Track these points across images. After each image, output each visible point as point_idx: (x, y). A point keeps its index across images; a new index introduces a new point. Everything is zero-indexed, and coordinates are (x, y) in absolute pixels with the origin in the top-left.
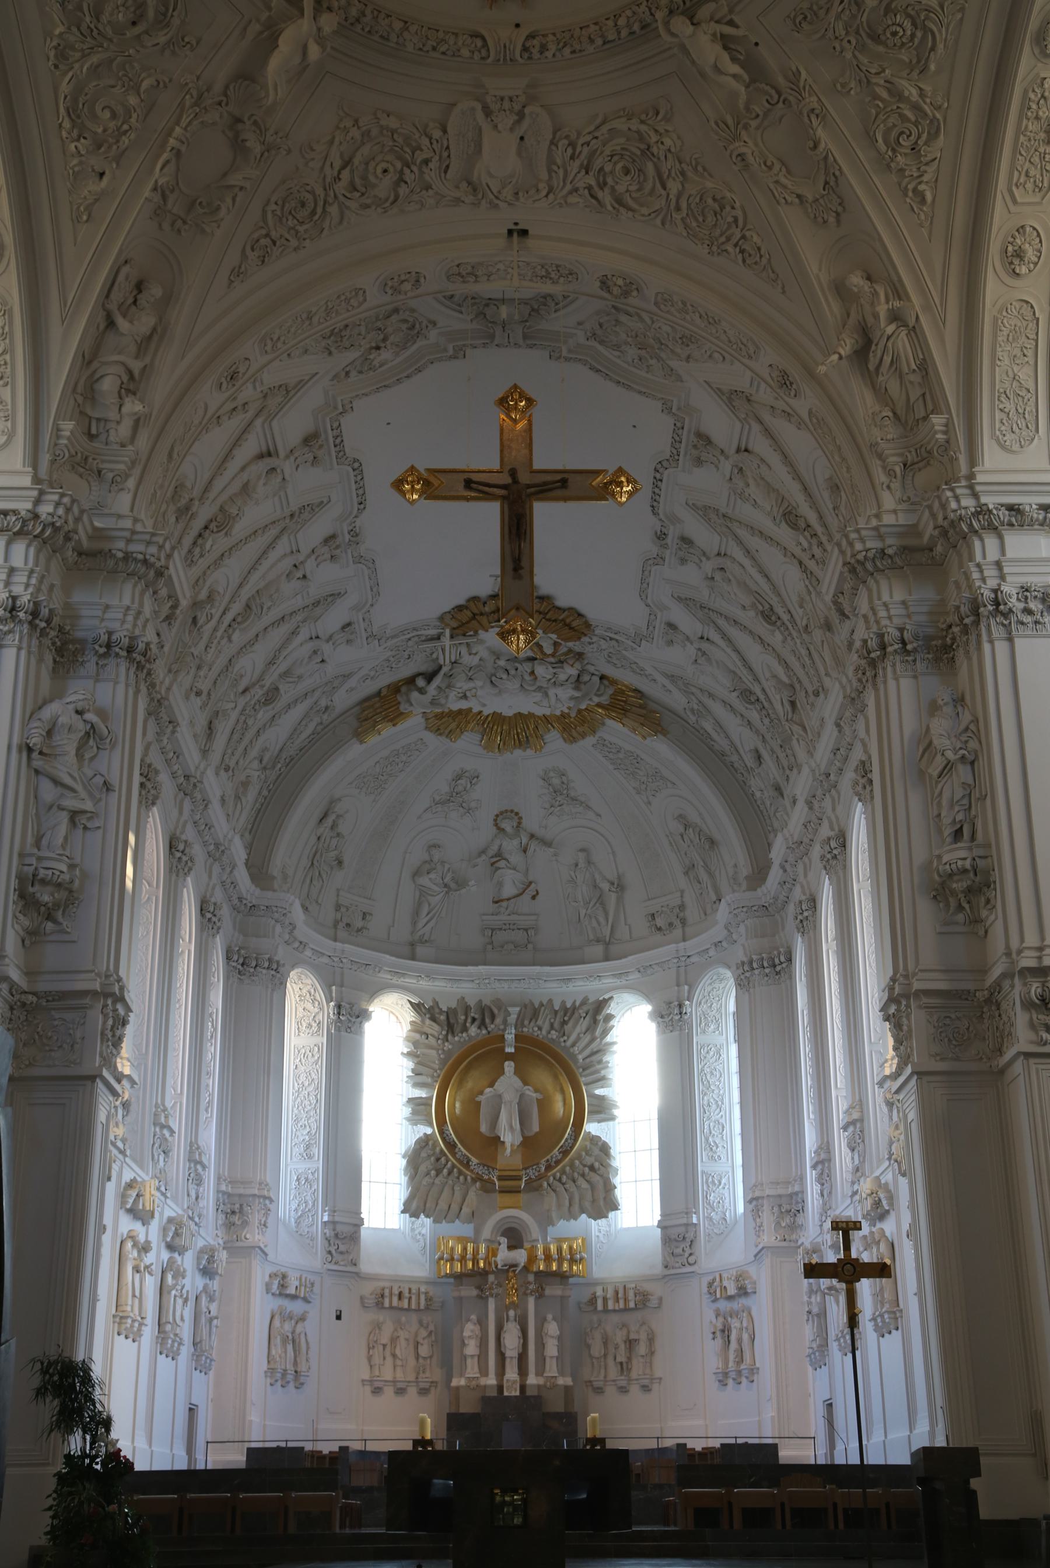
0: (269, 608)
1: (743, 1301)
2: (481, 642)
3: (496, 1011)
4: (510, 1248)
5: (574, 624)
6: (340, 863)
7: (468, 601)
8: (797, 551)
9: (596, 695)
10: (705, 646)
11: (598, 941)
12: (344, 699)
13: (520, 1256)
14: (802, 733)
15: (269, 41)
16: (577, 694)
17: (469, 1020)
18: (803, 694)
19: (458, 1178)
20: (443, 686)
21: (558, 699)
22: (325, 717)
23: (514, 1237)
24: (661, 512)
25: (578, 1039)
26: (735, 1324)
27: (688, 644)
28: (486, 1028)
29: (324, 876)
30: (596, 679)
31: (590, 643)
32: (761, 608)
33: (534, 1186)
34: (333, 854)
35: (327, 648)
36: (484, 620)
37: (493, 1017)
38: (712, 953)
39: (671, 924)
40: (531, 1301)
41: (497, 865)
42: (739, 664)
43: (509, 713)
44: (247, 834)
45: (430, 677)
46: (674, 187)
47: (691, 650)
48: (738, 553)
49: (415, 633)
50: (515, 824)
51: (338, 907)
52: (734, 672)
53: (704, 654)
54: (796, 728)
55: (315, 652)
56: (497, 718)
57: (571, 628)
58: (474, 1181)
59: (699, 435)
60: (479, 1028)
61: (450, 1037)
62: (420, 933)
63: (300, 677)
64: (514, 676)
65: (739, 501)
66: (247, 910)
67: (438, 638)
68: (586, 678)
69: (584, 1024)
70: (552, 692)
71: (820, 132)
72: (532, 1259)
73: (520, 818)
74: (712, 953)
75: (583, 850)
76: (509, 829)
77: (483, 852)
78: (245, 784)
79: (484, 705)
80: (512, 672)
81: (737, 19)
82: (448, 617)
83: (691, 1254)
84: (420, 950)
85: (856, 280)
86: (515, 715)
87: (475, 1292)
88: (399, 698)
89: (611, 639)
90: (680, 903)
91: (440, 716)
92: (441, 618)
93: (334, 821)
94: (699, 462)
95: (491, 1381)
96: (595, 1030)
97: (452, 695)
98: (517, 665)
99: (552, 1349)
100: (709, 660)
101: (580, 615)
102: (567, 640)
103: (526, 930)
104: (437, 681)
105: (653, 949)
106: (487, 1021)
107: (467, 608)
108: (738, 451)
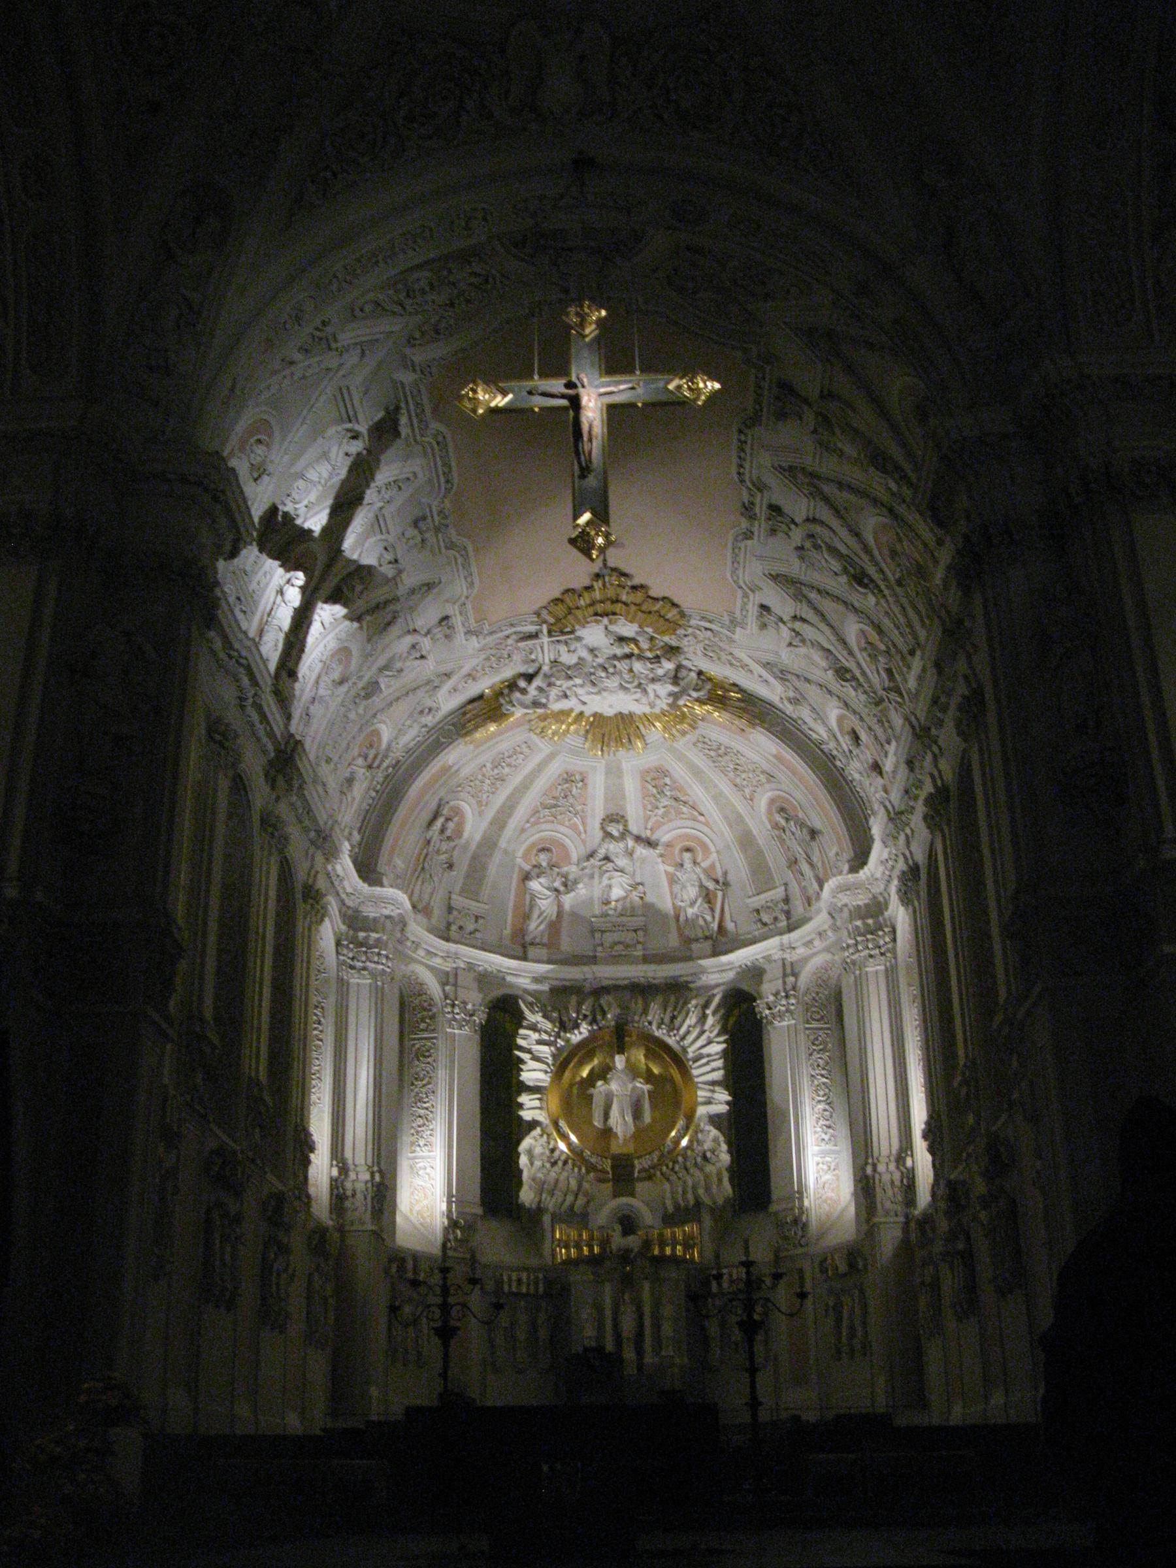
0: (362, 593)
2: (579, 639)
3: (606, 1008)
5: (669, 616)
6: (451, 866)
7: (563, 594)
8: (885, 498)
9: (694, 690)
10: (798, 625)
11: (706, 938)
12: (448, 702)
13: (633, 1241)
14: (899, 699)
16: (676, 689)
17: (581, 1017)
18: (898, 658)
19: (573, 1169)
20: (544, 686)
21: (657, 696)
22: (430, 718)
24: (747, 478)
25: (688, 1032)
26: (846, 1299)
27: (781, 625)
28: (597, 1024)
29: (436, 879)
30: (693, 675)
31: (686, 636)
32: (852, 571)
34: (443, 857)
35: (426, 644)
36: (578, 613)
37: (604, 1013)
38: (817, 943)
39: (776, 919)
40: (647, 1286)
41: (604, 868)
42: (832, 638)
43: (610, 712)
44: (355, 833)
45: (529, 678)
47: (785, 632)
48: (826, 514)
49: (514, 630)
50: (621, 828)
51: (450, 909)
52: (829, 651)
53: (798, 634)
54: (893, 696)
55: (413, 646)
56: (599, 719)
57: (667, 620)
58: (588, 1172)
60: (591, 1024)
61: (562, 1034)
62: (531, 936)
63: (400, 671)
64: (612, 674)
65: (825, 454)
67: (535, 636)
68: (683, 673)
69: (692, 1020)
70: (650, 688)
73: (626, 821)
74: (817, 943)
75: (688, 850)
76: (615, 833)
77: (591, 855)
78: (350, 781)
79: (584, 703)
80: (611, 670)
82: (544, 613)
83: (803, 1237)
84: (532, 952)
86: (616, 715)
88: (502, 701)
89: (706, 629)
90: (784, 897)
91: (543, 718)
92: (538, 614)
93: (443, 825)
94: (782, 415)
96: (703, 1024)
97: (554, 692)
98: (616, 663)
99: (667, 1329)
100: (803, 641)
101: (674, 605)
102: (663, 633)
103: (635, 931)
104: (538, 682)
105: (760, 941)
106: (599, 1017)
107: (562, 601)
108: (822, 397)
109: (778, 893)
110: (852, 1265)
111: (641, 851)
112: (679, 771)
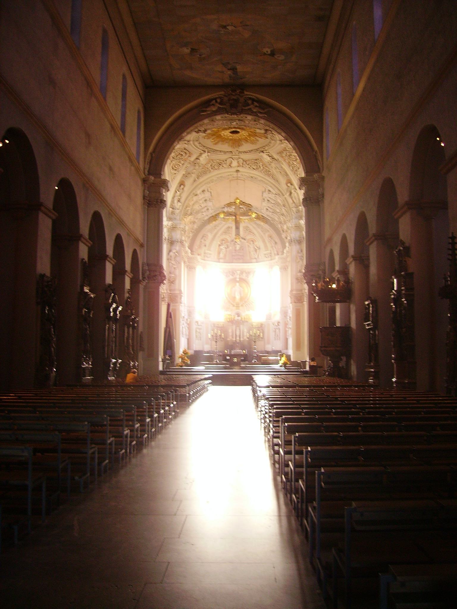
1: (279, 327)
4: (238, 316)
6: (205, 246)
11: (256, 259)
13: (239, 318)
15: (201, 154)
23: (239, 315)
33: (242, 306)
46: (262, 168)
59: (269, 191)
66: (189, 258)
71: (282, 165)
72: (242, 318)
75: (253, 241)
77: (232, 241)
81: (270, 152)
84: (221, 260)
85: (289, 185)
87: (231, 324)
92: (225, 206)
94: (269, 193)
95: (234, 339)
101: (251, 205)
109: (269, 252)
110: (278, 324)
111: (243, 241)
112: (251, 227)
